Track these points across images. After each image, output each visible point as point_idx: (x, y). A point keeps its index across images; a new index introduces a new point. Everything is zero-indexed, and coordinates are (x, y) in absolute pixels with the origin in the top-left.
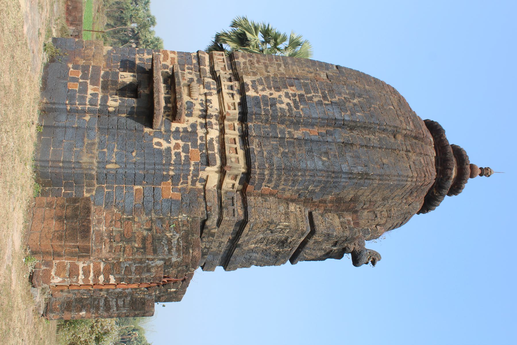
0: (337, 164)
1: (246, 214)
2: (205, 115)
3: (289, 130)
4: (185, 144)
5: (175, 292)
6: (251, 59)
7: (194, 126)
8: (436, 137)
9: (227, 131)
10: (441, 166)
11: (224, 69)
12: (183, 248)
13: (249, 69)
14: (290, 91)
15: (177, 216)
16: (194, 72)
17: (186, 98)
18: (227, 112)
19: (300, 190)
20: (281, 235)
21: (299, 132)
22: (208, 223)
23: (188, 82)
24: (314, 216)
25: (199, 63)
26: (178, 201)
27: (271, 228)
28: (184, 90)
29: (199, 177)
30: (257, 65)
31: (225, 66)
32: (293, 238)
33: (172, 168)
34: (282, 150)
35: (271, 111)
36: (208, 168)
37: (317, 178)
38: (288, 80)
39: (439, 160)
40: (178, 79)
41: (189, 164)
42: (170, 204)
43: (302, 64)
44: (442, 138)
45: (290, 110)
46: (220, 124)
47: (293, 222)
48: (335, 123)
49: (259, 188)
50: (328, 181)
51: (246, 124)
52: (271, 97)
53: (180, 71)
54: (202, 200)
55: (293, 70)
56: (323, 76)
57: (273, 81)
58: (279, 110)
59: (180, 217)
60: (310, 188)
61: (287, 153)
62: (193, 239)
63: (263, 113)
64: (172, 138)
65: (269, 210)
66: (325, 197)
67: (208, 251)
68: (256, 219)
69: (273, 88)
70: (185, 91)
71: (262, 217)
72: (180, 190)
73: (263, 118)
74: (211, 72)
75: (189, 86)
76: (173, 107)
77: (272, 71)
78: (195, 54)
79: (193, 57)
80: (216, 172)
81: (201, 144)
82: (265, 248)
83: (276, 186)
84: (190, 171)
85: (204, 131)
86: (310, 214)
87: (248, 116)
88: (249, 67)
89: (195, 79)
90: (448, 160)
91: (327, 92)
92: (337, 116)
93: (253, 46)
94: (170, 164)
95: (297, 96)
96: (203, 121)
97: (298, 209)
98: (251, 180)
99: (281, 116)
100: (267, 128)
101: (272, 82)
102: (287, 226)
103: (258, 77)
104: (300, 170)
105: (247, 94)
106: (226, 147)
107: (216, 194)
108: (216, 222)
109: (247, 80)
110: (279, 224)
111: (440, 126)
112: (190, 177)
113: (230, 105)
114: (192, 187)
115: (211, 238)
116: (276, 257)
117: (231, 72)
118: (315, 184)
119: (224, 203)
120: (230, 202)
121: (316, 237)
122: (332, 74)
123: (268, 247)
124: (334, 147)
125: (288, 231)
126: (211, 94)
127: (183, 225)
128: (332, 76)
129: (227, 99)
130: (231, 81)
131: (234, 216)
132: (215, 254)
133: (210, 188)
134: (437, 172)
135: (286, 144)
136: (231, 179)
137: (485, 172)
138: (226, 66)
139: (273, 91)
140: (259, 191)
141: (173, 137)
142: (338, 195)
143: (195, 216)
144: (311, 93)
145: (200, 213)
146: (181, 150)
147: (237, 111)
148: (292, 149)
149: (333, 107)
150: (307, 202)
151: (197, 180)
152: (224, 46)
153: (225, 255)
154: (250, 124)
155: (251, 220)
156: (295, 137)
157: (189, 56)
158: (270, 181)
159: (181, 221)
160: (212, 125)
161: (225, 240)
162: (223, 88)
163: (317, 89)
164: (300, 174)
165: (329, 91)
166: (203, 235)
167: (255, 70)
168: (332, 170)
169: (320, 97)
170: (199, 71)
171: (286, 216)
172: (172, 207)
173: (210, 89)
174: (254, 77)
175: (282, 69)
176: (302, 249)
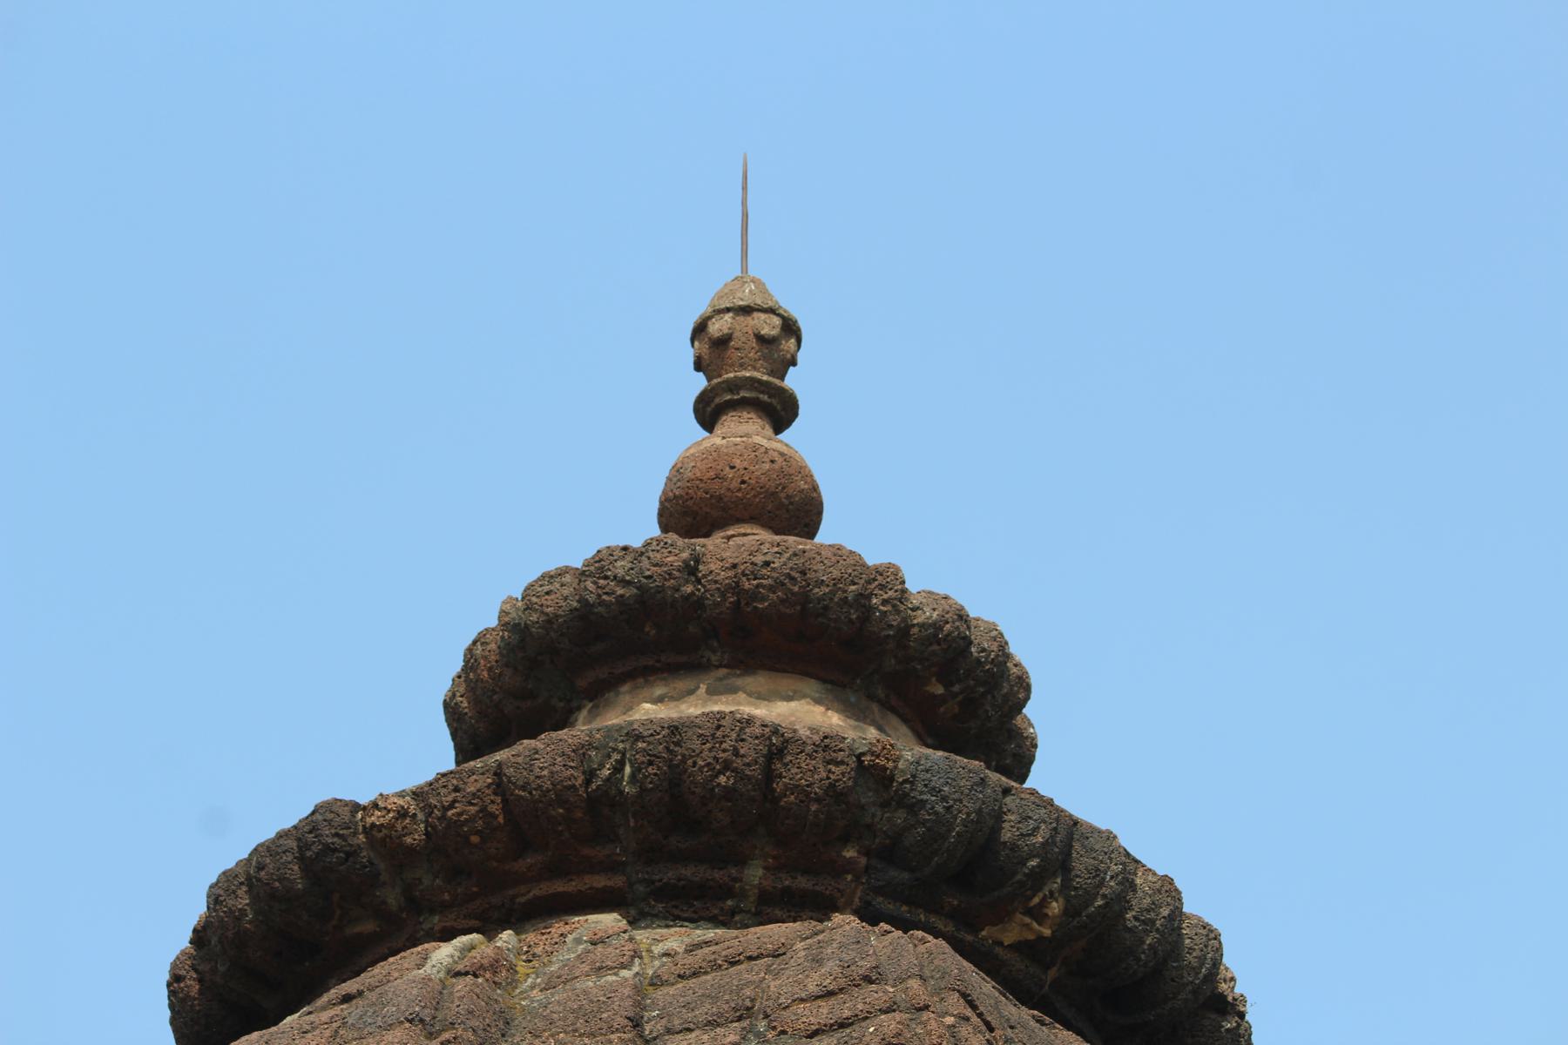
8: (392, 898)
10: (742, 862)
39: (669, 874)
44: (415, 837)
90: (675, 776)
111: (266, 851)
134: (820, 907)
137: (747, 368)
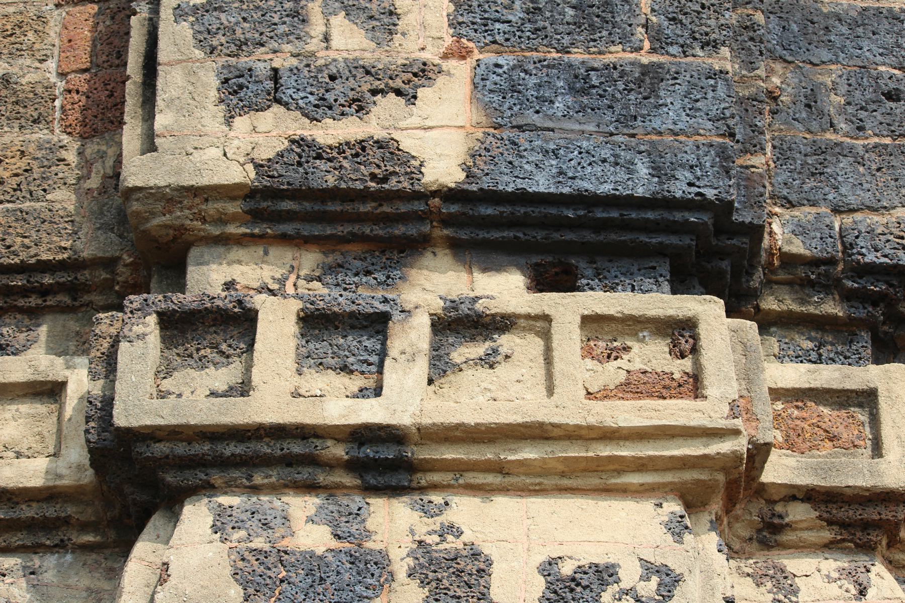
51: (769, 283)
130: (234, 323)
162: (371, 412)
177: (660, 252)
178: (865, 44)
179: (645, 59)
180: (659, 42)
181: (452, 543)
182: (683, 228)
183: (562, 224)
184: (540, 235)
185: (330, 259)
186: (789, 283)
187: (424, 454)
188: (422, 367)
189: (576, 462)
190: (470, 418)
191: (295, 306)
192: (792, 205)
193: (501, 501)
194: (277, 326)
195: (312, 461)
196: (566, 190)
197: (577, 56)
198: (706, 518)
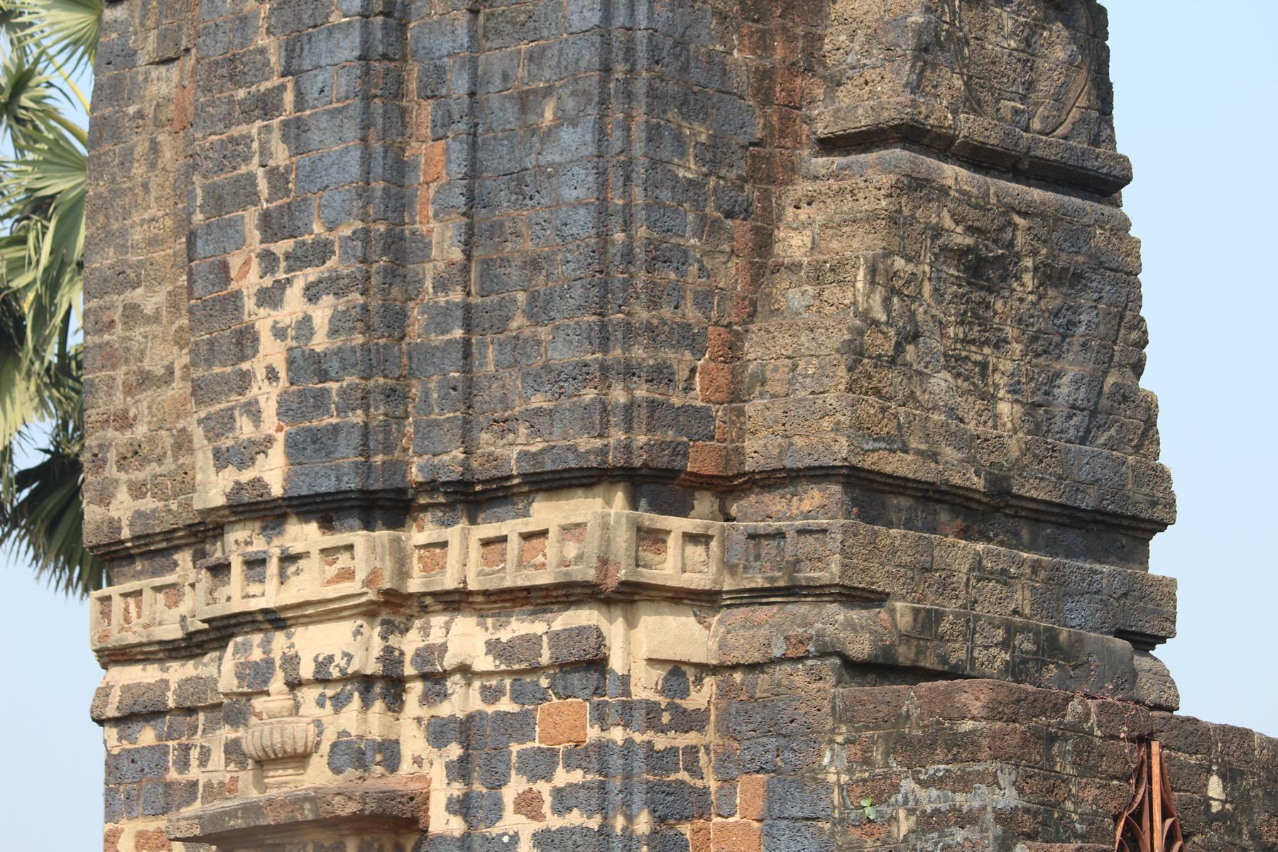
0: (570, 52)
1: (819, 474)
2: (386, 685)
3: (429, 284)
4: (518, 770)
5: (1229, 776)
6: (112, 456)
7: (438, 733)
9: (449, 582)
11: (173, 592)
12: (955, 759)
13: (162, 469)
14: (250, 281)
15: (828, 788)
16: (198, 739)
17: (317, 775)
18: (368, 582)
19: (703, 218)
20: (927, 288)
21: (435, 238)
22: (861, 648)
23: (242, 765)
24: (837, 129)
25: (153, 714)
26: (769, 789)
27: (888, 349)
28: (279, 785)
29: (657, 698)
30: (141, 430)
31: (157, 589)
32: (948, 223)
33: (619, 822)
34: (518, 321)
35: (351, 380)
36: (616, 664)
37: (638, 149)
38: (198, 290)
40: (232, 813)
41: (602, 748)
42: (783, 823)
43: (116, 193)
45: (332, 285)
46: (425, 610)
47: (861, 244)
48: (385, 57)
49: (703, 416)
50: (652, 93)
52: (283, 374)
53: (196, 807)
54: (763, 680)
55: (153, 242)
56: (163, 83)
57: (209, 363)
58: (339, 341)
59: (832, 778)
60: (688, 170)
61: (533, 298)
62: (920, 717)
63: (358, 417)
64: (495, 830)
65: (802, 364)
66: (741, 81)
67: (1025, 629)
68: (837, 428)
69: (245, 366)
70: (285, 783)
71: (831, 398)
72: (727, 781)
73: (379, 414)
74: (191, 657)
75: (265, 761)
76: (359, 832)
77: (162, 354)
78: (112, 732)
79: (126, 745)
80: (631, 624)
81: (515, 698)
82: (1018, 347)
83: (690, 339)
84: (629, 742)
85: (454, 684)
86: (830, 145)
87: (378, 486)
88: (154, 468)
89: (227, 733)
91: (241, 94)
92: (348, 48)
93: (17, 267)
94: (604, 832)
95: (273, 247)
96: (416, 689)
97: (803, 214)
98: (663, 461)
99: (368, 329)
100: (427, 393)
101: (217, 370)
102: (873, 271)
103: (198, 433)
104: (603, 237)
105: (277, 491)
106: (520, 583)
107: (740, 614)
108: (857, 615)
109: (214, 489)
110: (865, 315)
112: (661, 742)
113: (332, 571)
114: (711, 728)
115: (944, 627)
116: (1078, 277)
117: (184, 558)
118: (665, 155)
119: (772, 579)
120: (768, 547)
121: (938, 112)
122: (153, 35)
123: (1010, 331)
124: (494, 60)
125: (899, 263)
126: (291, 661)
127: (867, 762)
128: (162, 37)
129: (307, 584)
131: (824, 531)
132: (1056, 590)
133: (713, 645)
135: (496, 298)
136: (658, 552)
138: (158, 581)
139: (257, 366)
140: (719, 412)
141: (492, 823)
142: (723, 17)
143: (827, 709)
144: (251, 177)
145: (815, 688)
146: (543, 788)
147: (358, 538)
148: (514, 273)
149: (307, 65)
150: (767, 170)
151: (672, 707)
152: (28, 457)
153: (1070, 535)
154: (415, 474)
155: (840, 450)
156: (457, 255)
157: (125, 765)
158: (661, 375)
159: (850, 771)
160: (429, 649)
161: (960, 553)
163: (232, 140)
164: (619, 237)
165: (235, 78)
166: (930, 662)
167: (167, 440)
168: (595, 77)
169: (268, 129)
170: (191, 711)
171: (830, 276)
172: (796, 812)
173: (269, 663)
174: (200, 455)
175: (151, 300)
176: (1019, 159)
177: (352, 507)
178: (446, 361)
179: (334, 421)
180: (341, 411)
181: (292, 652)
182: (352, 499)
183: (316, 503)
184: (315, 508)
185: (264, 524)
186: (426, 491)
187: (283, 616)
188: (275, 581)
189: (326, 612)
190: (289, 602)
191: (241, 559)
192: (420, 456)
193: (311, 627)
194: (237, 569)
195: (254, 622)
196: (312, 492)
197: (315, 423)
198: (379, 620)
